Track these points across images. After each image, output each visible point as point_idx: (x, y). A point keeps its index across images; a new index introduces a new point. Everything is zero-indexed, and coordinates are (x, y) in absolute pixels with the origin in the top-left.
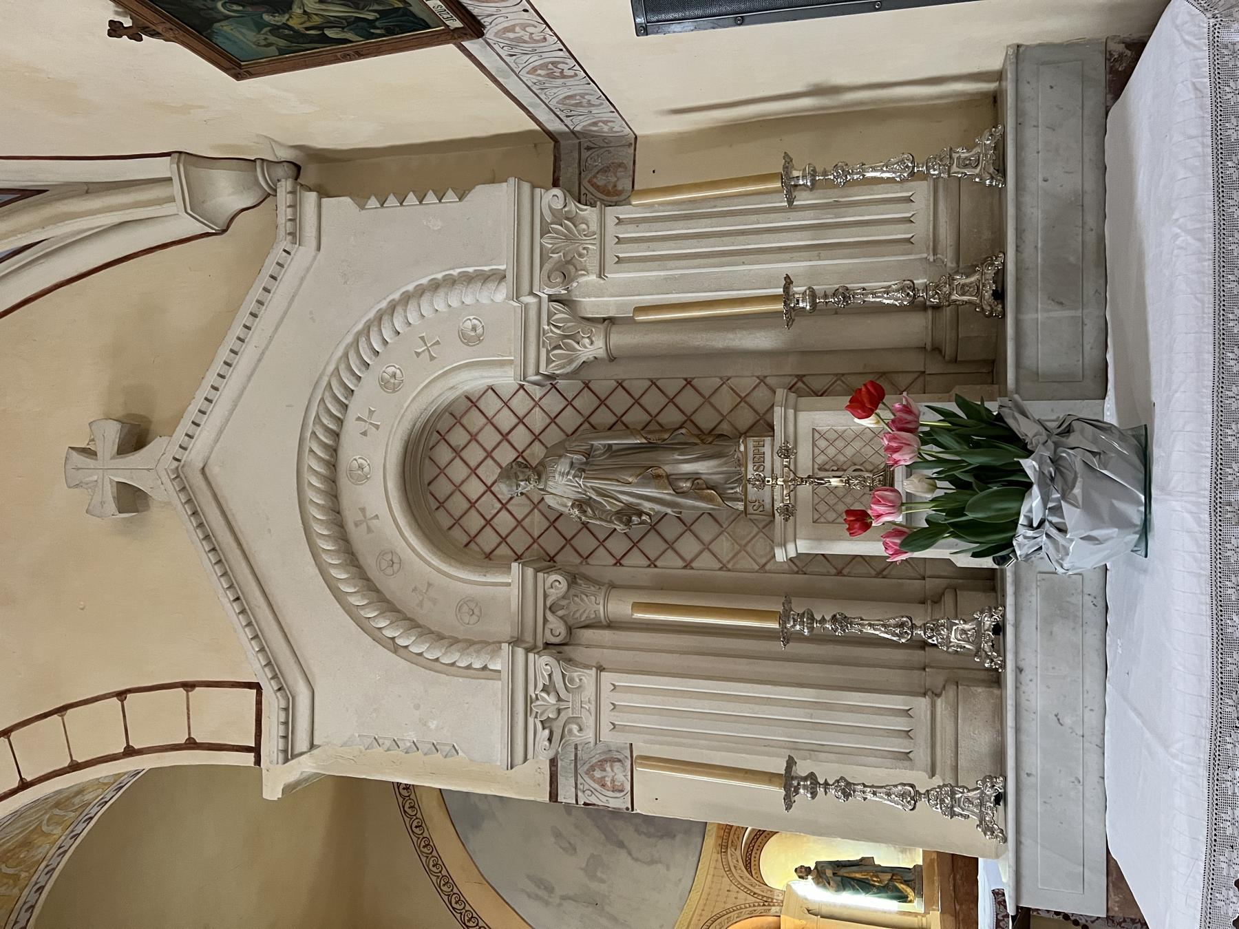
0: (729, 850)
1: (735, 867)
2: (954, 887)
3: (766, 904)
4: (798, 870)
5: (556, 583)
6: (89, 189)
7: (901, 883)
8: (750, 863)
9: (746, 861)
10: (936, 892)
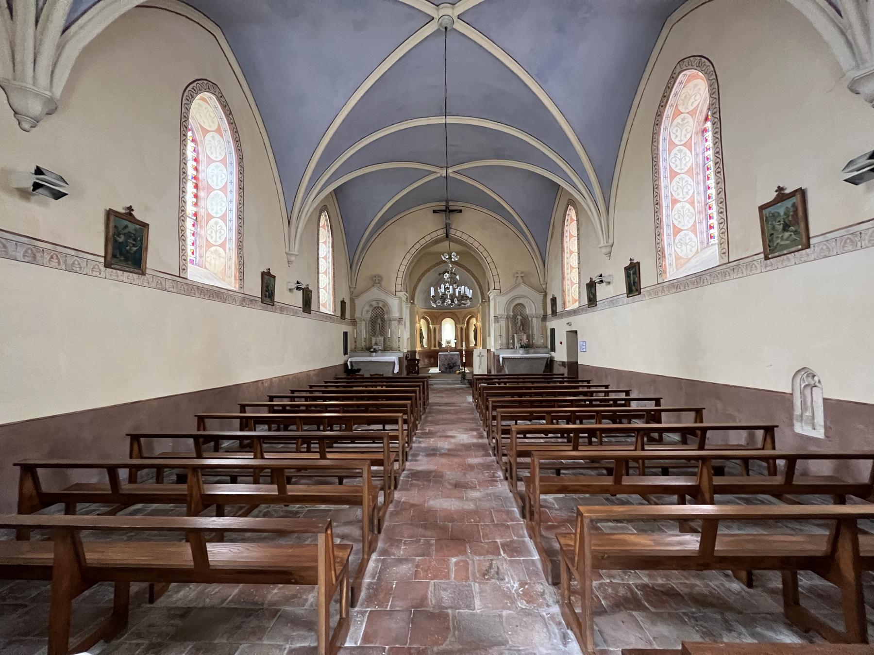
5: (511, 317)
6: (544, 271)
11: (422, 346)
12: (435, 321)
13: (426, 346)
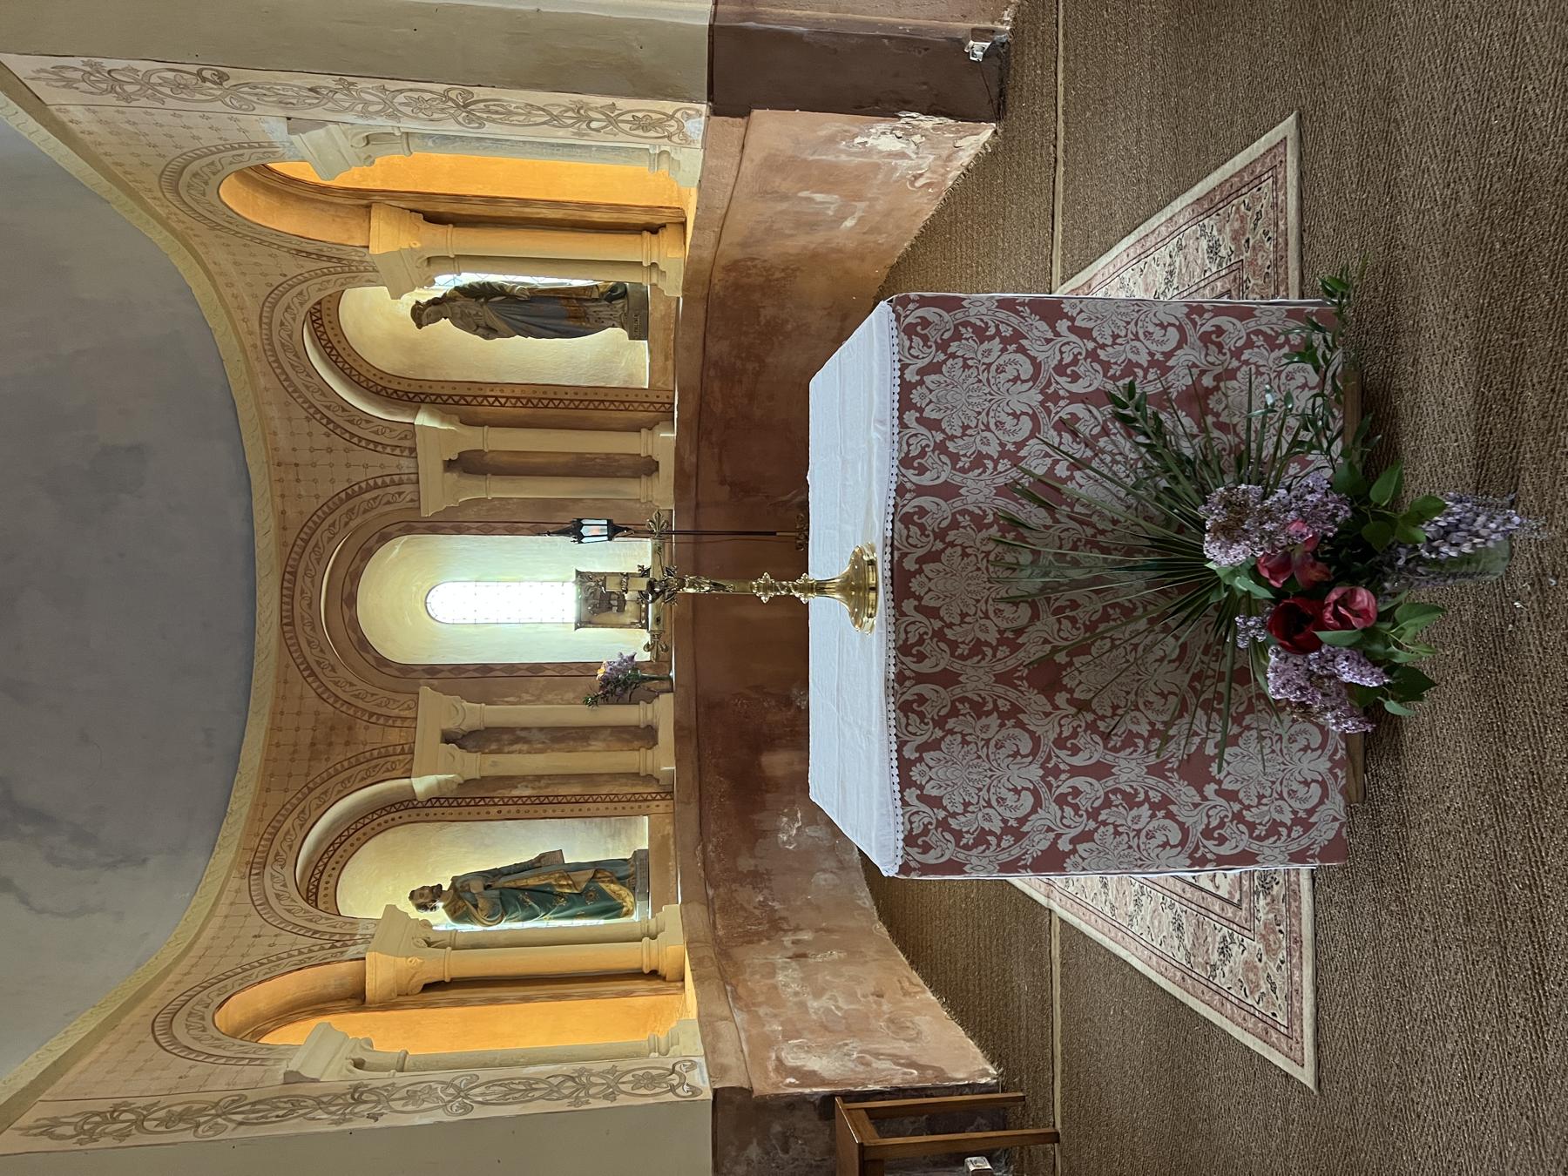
0: (268, 868)
1: (278, 896)
2: (704, 863)
3: (338, 944)
4: (416, 894)
7: (612, 882)
8: (316, 894)
9: (308, 890)
10: (672, 884)
11: (631, 873)
12: (372, 737)
13: (636, 837)
